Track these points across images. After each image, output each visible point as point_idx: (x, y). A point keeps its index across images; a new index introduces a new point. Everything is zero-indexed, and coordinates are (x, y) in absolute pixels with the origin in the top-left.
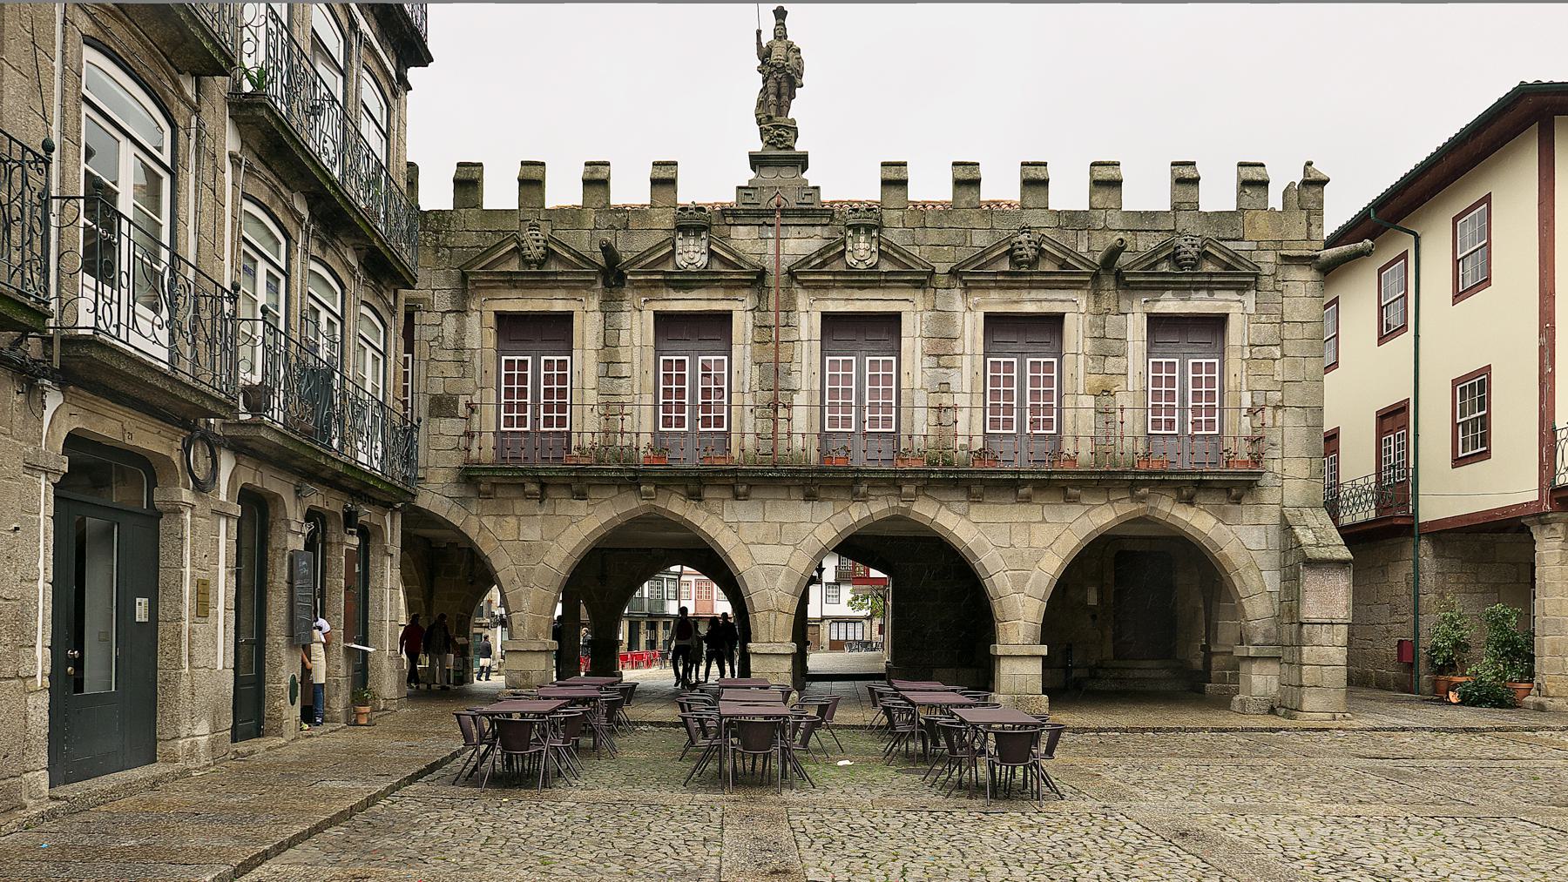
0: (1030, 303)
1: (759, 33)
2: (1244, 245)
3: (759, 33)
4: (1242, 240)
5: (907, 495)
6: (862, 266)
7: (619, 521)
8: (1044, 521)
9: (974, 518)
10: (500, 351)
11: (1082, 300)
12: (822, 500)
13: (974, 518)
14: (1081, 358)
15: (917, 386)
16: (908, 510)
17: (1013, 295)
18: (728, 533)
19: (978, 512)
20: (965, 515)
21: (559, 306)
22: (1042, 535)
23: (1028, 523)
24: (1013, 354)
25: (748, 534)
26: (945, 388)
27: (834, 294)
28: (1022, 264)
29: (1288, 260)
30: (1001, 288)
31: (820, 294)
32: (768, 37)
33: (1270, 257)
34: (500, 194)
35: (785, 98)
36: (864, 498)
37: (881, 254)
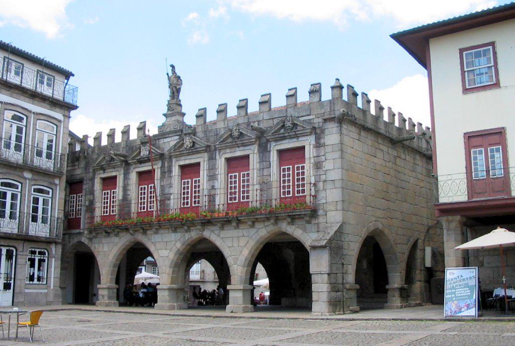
0: (239, 153)
1: (168, 74)
2: (311, 117)
3: (168, 74)
4: (310, 115)
5: (198, 229)
6: (188, 148)
7: (128, 243)
10: (103, 190)
12: (177, 232)
13: (221, 236)
14: (255, 171)
16: (202, 234)
17: (233, 150)
18: (153, 246)
19: (224, 234)
20: (219, 236)
21: (114, 174)
22: (243, 242)
23: (238, 237)
24: (236, 172)
25: (158, 246)
26: (213, 188)
27: (182, 158)
28: (235, 138)
29: (325, 120)
30: (230, 148)
31: (178, 159)
32: (170, 74)
33: (320, 120)
34: (104, 142)
35: (176, 93)
36: (188, 230)
37: (194, 143)
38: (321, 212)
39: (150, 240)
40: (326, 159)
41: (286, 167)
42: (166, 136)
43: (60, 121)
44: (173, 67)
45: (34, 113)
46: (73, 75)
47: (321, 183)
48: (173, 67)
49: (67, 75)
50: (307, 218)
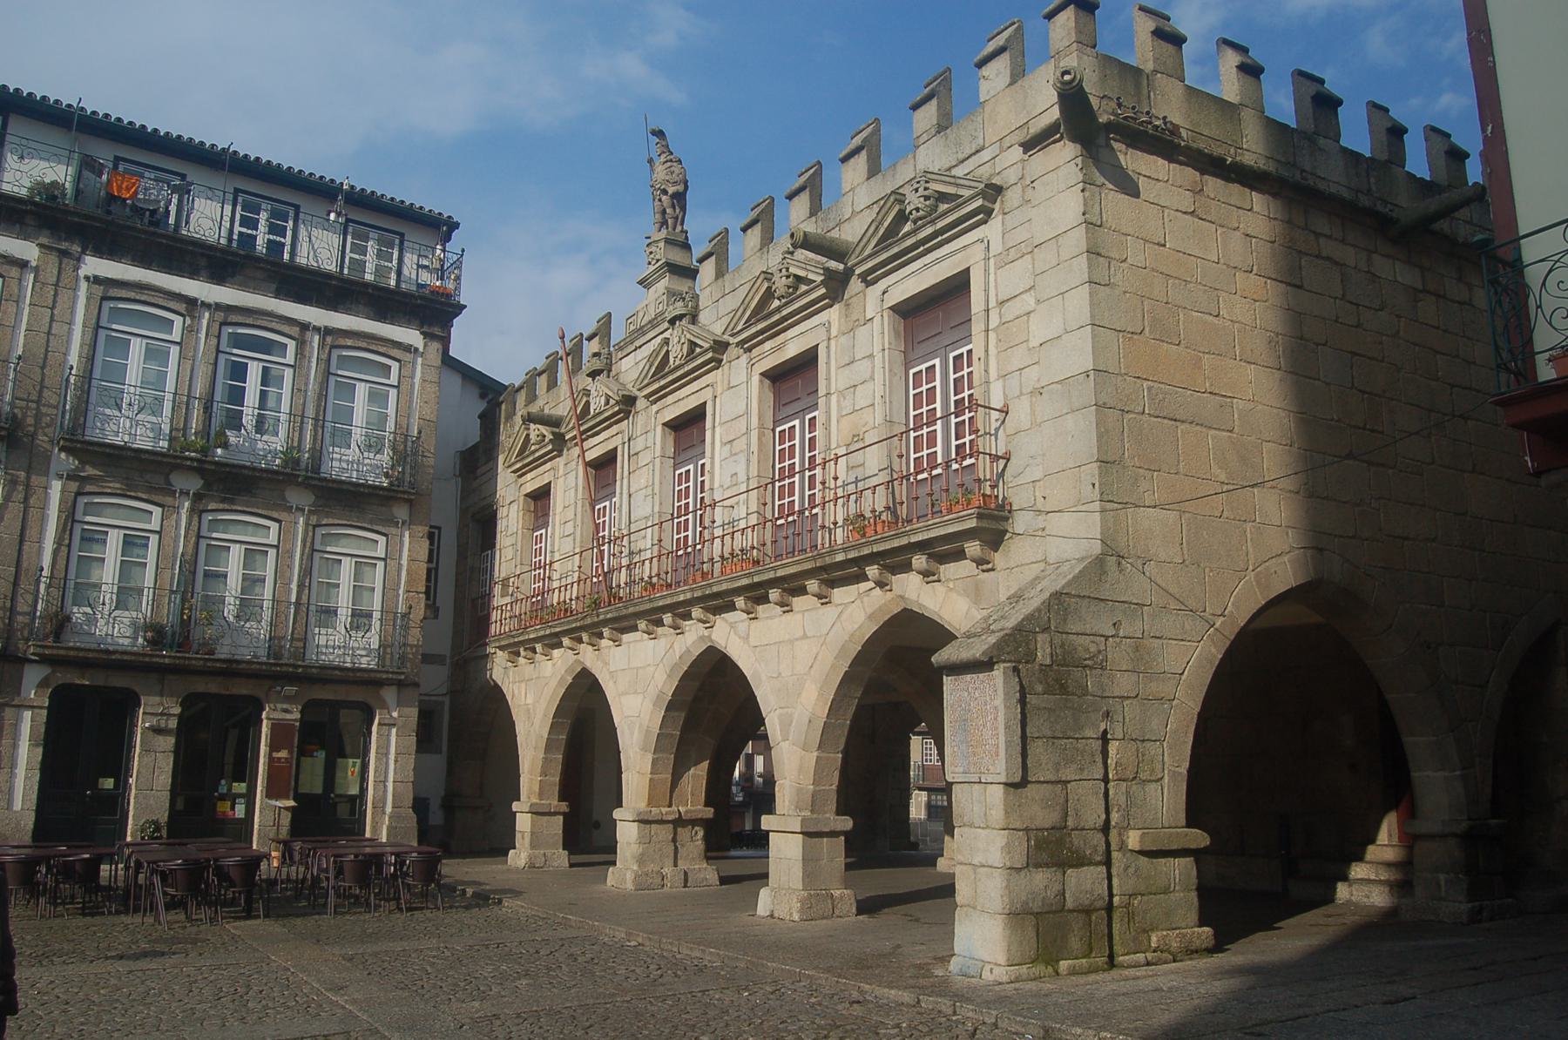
8: (805, 637)
9: (753, 641)
11: (833, 314)
15: (716, 485)
18: (611, 684)
38: (1020, 523)
39: (606, 664)
40: (1038, 302)
41: (923, 367)
42: (637, 343)
43: (408, 348)
44: (659, 134)
45: (317, 329)
46: (457, 225)
47: (1025, 400)
48: (659, 134)
49: (440, 227)
50: (973, 548)
